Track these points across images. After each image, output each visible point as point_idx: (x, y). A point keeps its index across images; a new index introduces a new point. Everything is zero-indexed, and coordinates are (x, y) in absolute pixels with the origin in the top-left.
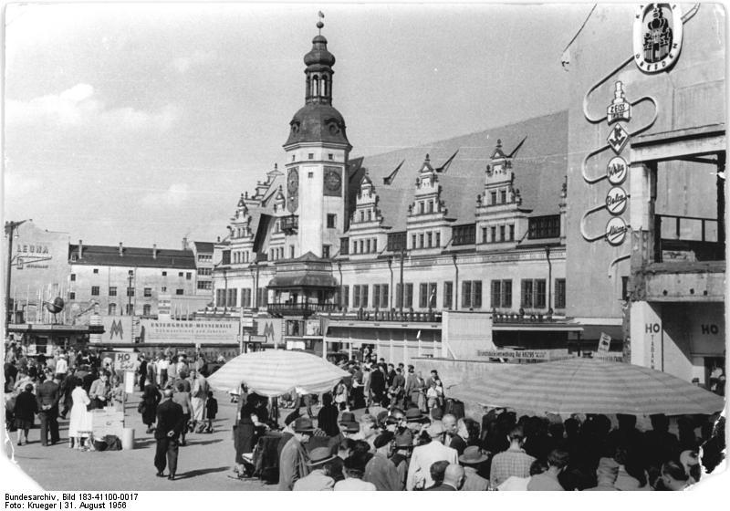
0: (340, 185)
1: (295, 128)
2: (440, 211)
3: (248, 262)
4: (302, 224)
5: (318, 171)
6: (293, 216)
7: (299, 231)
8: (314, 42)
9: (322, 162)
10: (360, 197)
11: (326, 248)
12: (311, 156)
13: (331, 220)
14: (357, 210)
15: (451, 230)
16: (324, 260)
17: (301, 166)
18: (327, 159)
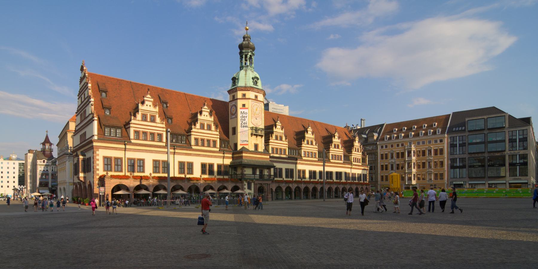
10: (276, 127)
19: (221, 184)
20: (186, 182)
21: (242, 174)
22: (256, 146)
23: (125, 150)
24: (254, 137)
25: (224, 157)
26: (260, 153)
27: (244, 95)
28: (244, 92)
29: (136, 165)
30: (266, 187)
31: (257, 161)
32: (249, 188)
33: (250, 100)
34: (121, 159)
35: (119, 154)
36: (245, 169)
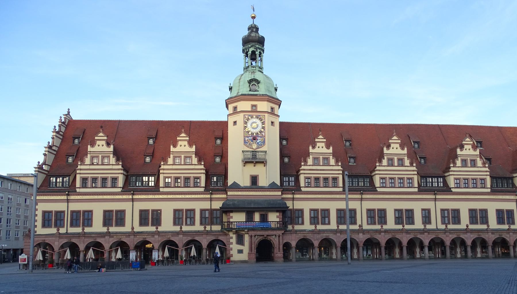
3: (114, 186)
8: (249, 29)
10: (314, 147)
14: (311, 156)
17: (266, 115)
19: (190, 238)
20: (132, 237)
21: (229, 222)
22: (254, 179)
23: (68, 201)
24: (250, 167)
25: (211, 199)
26: (263, 189)
27: (235, 108)
28: (234, 105)
29: (84, 218)
30: (275, 241)
31: (239, 201)
32: (240, 241)
33: (242, 115)
34: (64, 212)
35: (61, 207)
36: (231, 214)
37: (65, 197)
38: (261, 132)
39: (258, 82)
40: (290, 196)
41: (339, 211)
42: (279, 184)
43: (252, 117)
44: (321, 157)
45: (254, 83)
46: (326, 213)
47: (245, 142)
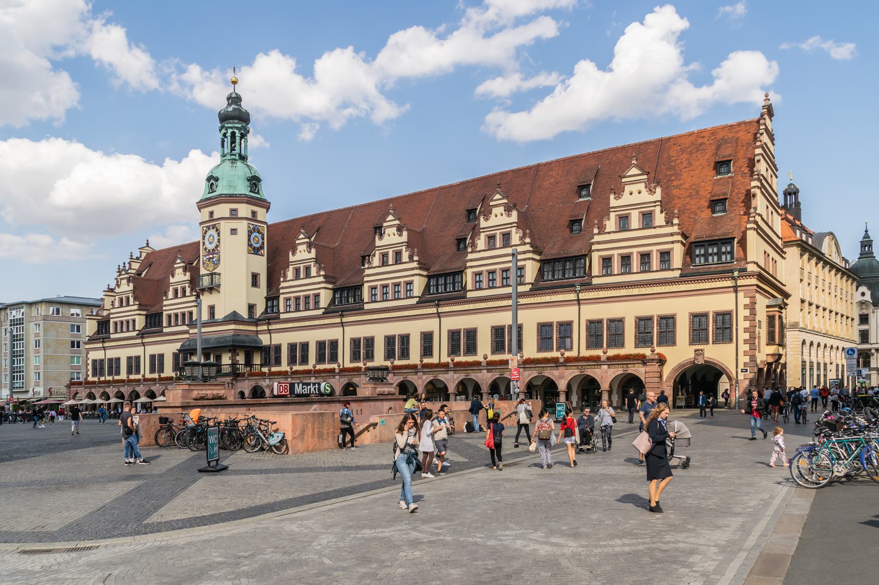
0: (263, 243)
1: (212, 184)
2: (411, 257)
3: (134, 330)
4: (225, 281)
5: (243, 227)
6: (212, 275)
7: (222, 289)
9: (247, 219)
10: (293, 254)
11: (251, 308)
12: (234, 211)
13: (255, 280)
14: (291, 268)
15: (426, 280)
16: (251, 320)
17: (222, 222)
18: (250, 216)
23: (104, 348)
37: (100, 345)
38: (217, 246)
39: (217, 179)
40: (265, 327)
41: (321, 345)
42: (245, 315)
43: (208, 227)
44: (302, 265)
45: (212, 181)
46: (305, 346)
47: (204, 264)
